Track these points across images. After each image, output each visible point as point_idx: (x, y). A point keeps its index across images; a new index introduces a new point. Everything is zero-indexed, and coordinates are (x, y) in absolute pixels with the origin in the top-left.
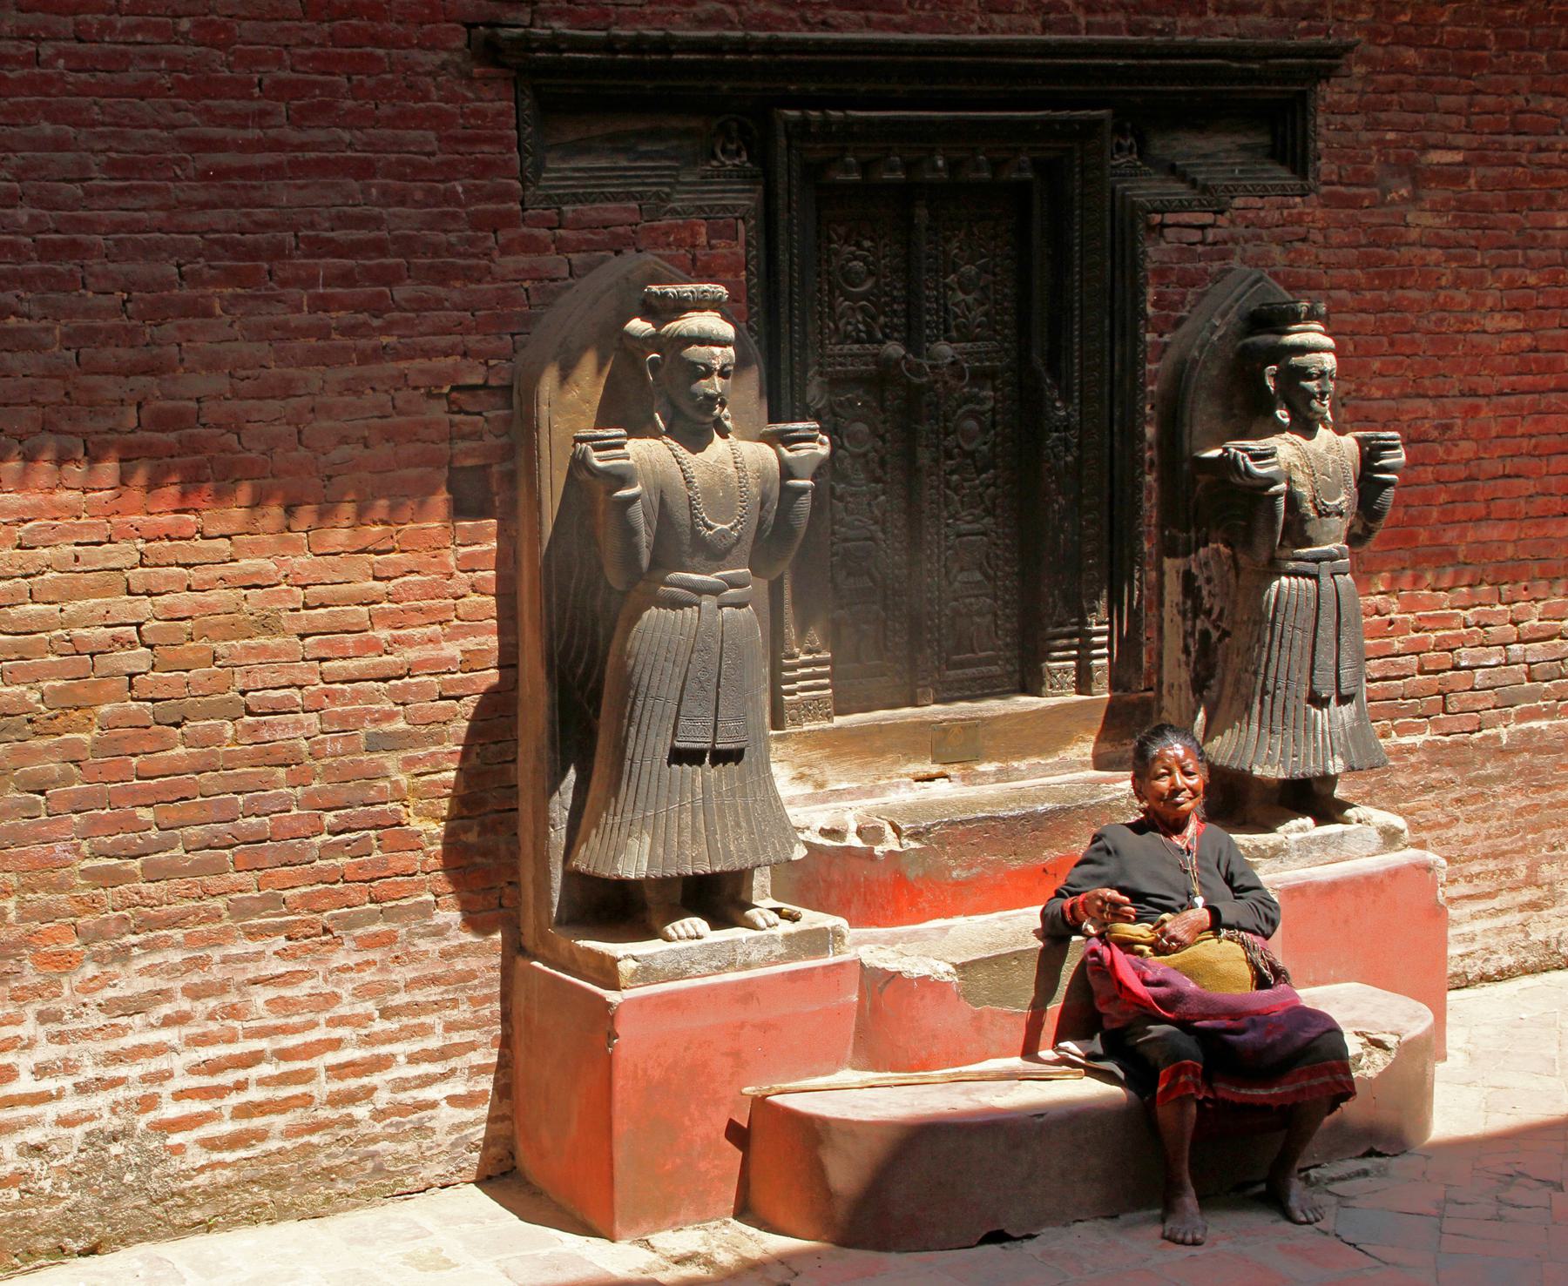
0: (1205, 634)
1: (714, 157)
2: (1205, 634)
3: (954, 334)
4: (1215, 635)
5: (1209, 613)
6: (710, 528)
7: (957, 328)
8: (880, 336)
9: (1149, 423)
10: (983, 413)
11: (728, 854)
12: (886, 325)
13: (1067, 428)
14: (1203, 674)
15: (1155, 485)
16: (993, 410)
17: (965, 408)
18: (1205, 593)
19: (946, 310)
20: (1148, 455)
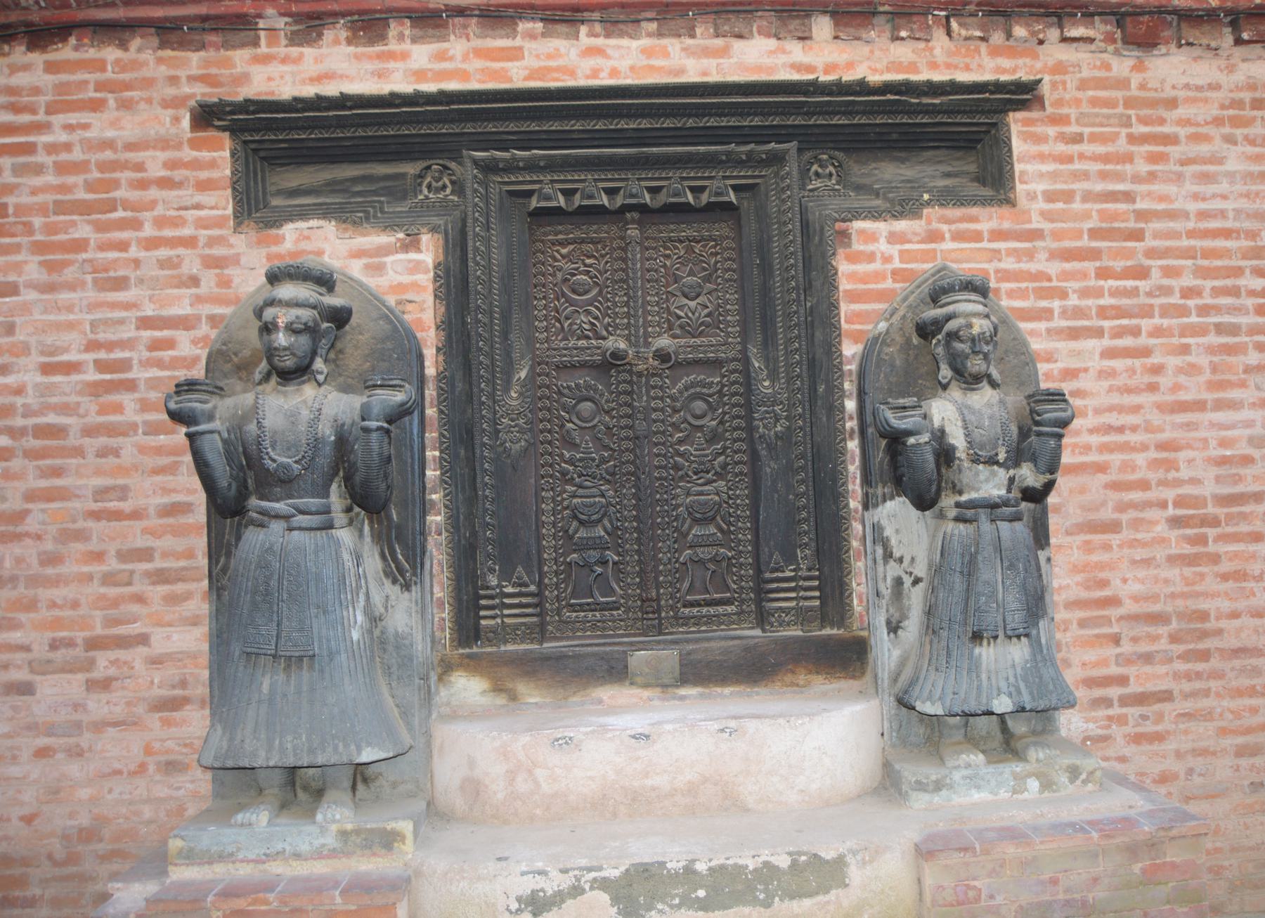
0: (899, 582)
1: (421, 191)
2: (899, 582)
3: (678, 332)
4: (908, 581)
5: (901, 560)
6: (274, 461)
7: (681, 327)
8: (605, 333)
9: (850, 397)
10: (710, 396)
11: (282, 750)
12: (609, 325)
13: (774, 403)
14: (897, 615)
15: (857, 451)
16: (720, 392)
17: (692, 391)
18: (893, 542)
19: (669, 313)
20: (849, 425)
